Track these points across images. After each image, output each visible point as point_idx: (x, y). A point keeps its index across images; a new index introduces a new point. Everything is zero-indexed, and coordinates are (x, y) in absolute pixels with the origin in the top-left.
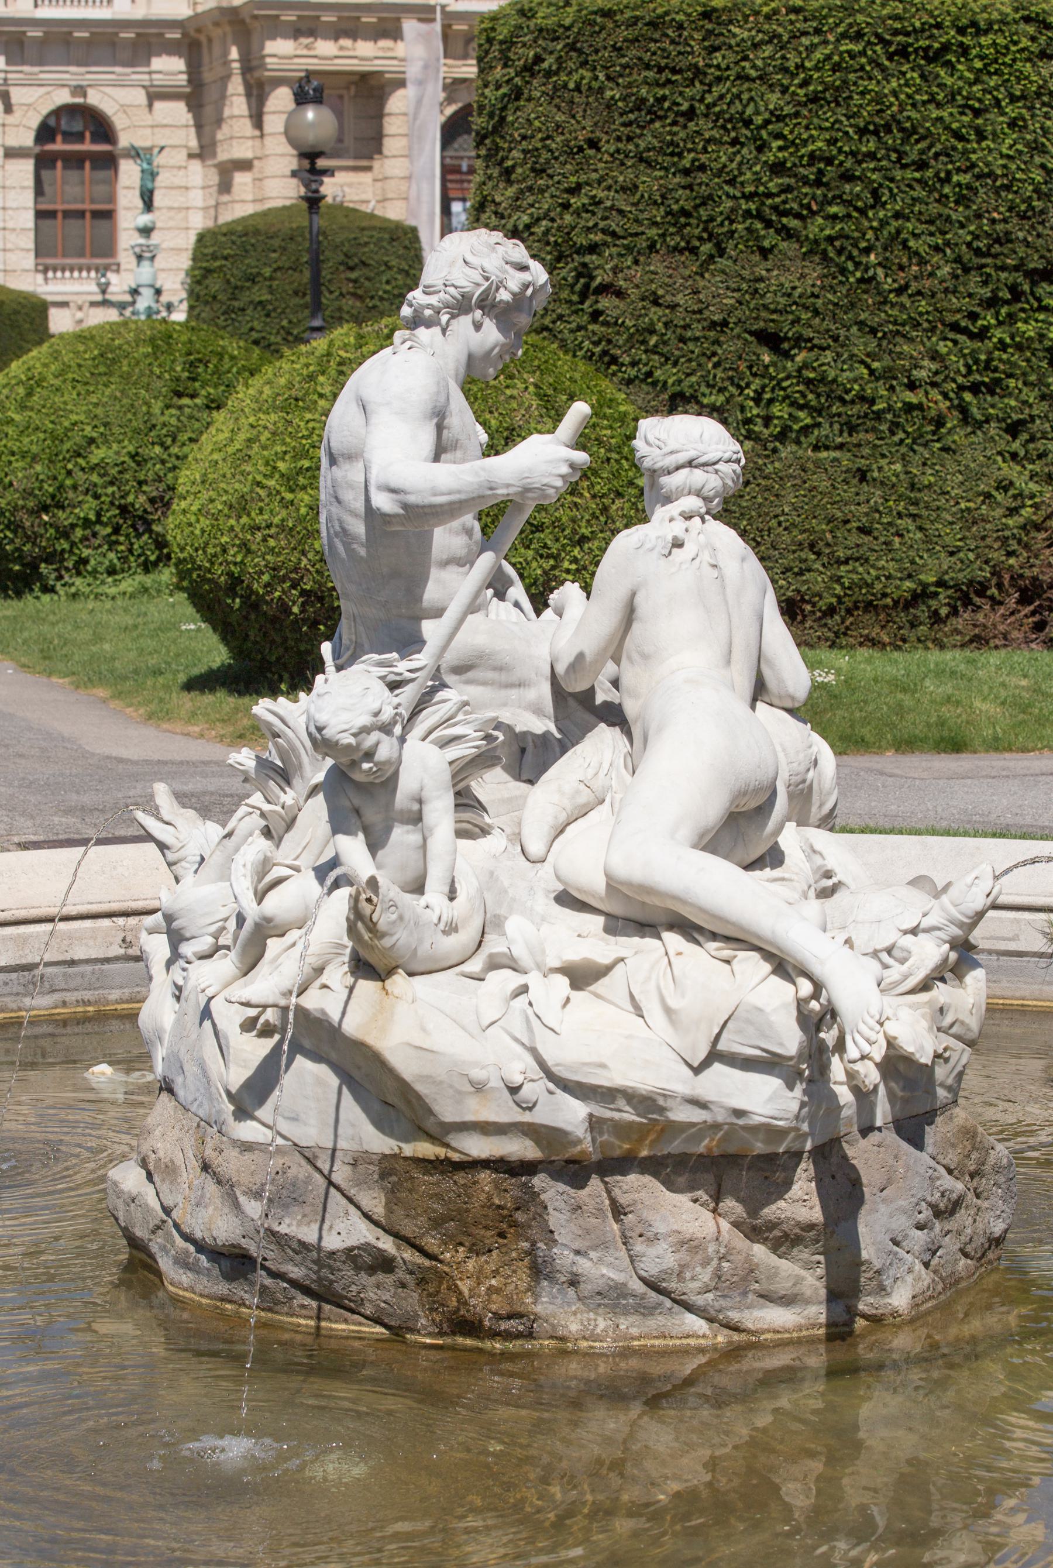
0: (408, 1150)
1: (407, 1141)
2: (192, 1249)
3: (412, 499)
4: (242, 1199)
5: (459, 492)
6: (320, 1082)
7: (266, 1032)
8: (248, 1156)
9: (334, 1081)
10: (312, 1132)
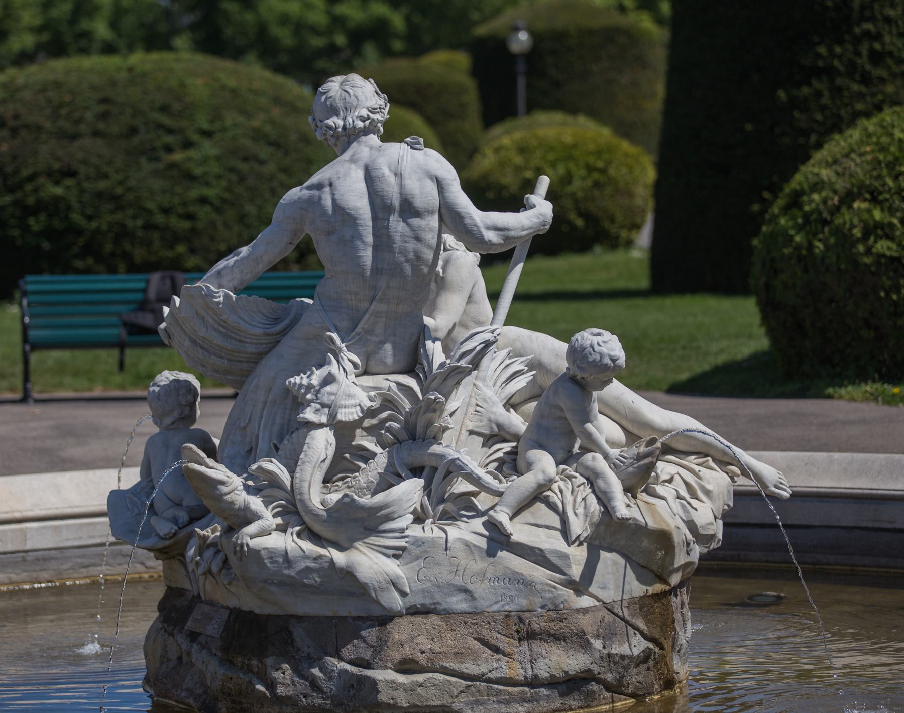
0: (651, 590)
1: (650, 585)
2: (527, 689)
3: (512, 234)
4: (592, 641)
5: (531, 228)
6: (615, 563)
7: (581, 544)
8: (587, 616)
9: (622, 561)
10: (610, 595)
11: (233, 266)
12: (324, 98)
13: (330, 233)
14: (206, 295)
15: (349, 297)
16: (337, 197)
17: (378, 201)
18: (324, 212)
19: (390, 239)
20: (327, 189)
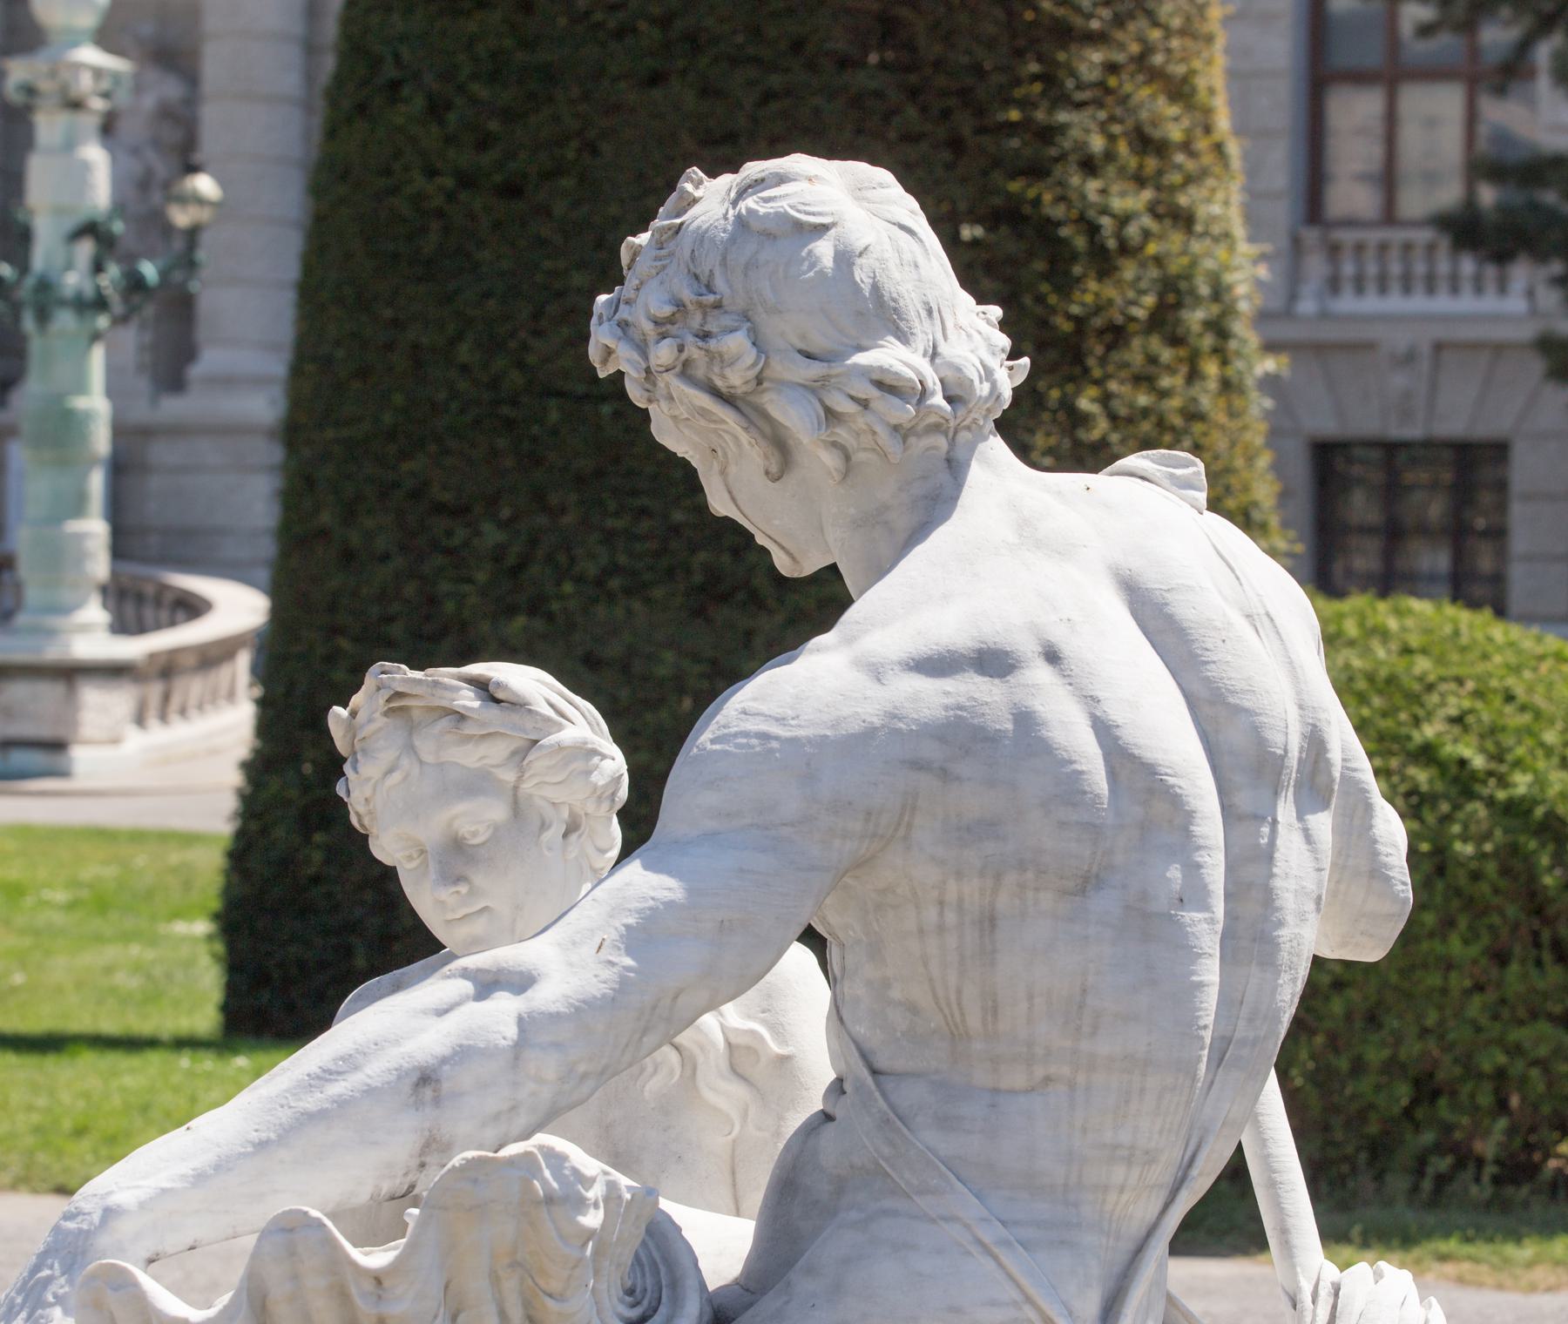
11: (520, 1045)
12: (824, 249)
13: (1088, 883)
14: (550, 1200)
15: (1118, 1174)
16: (1115, 713)
17: (1234, 736)
18: (1070, 786)
19: (1268, 898)
20: (1041, 673)
